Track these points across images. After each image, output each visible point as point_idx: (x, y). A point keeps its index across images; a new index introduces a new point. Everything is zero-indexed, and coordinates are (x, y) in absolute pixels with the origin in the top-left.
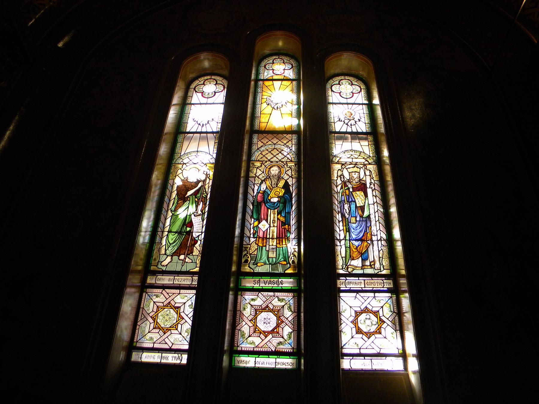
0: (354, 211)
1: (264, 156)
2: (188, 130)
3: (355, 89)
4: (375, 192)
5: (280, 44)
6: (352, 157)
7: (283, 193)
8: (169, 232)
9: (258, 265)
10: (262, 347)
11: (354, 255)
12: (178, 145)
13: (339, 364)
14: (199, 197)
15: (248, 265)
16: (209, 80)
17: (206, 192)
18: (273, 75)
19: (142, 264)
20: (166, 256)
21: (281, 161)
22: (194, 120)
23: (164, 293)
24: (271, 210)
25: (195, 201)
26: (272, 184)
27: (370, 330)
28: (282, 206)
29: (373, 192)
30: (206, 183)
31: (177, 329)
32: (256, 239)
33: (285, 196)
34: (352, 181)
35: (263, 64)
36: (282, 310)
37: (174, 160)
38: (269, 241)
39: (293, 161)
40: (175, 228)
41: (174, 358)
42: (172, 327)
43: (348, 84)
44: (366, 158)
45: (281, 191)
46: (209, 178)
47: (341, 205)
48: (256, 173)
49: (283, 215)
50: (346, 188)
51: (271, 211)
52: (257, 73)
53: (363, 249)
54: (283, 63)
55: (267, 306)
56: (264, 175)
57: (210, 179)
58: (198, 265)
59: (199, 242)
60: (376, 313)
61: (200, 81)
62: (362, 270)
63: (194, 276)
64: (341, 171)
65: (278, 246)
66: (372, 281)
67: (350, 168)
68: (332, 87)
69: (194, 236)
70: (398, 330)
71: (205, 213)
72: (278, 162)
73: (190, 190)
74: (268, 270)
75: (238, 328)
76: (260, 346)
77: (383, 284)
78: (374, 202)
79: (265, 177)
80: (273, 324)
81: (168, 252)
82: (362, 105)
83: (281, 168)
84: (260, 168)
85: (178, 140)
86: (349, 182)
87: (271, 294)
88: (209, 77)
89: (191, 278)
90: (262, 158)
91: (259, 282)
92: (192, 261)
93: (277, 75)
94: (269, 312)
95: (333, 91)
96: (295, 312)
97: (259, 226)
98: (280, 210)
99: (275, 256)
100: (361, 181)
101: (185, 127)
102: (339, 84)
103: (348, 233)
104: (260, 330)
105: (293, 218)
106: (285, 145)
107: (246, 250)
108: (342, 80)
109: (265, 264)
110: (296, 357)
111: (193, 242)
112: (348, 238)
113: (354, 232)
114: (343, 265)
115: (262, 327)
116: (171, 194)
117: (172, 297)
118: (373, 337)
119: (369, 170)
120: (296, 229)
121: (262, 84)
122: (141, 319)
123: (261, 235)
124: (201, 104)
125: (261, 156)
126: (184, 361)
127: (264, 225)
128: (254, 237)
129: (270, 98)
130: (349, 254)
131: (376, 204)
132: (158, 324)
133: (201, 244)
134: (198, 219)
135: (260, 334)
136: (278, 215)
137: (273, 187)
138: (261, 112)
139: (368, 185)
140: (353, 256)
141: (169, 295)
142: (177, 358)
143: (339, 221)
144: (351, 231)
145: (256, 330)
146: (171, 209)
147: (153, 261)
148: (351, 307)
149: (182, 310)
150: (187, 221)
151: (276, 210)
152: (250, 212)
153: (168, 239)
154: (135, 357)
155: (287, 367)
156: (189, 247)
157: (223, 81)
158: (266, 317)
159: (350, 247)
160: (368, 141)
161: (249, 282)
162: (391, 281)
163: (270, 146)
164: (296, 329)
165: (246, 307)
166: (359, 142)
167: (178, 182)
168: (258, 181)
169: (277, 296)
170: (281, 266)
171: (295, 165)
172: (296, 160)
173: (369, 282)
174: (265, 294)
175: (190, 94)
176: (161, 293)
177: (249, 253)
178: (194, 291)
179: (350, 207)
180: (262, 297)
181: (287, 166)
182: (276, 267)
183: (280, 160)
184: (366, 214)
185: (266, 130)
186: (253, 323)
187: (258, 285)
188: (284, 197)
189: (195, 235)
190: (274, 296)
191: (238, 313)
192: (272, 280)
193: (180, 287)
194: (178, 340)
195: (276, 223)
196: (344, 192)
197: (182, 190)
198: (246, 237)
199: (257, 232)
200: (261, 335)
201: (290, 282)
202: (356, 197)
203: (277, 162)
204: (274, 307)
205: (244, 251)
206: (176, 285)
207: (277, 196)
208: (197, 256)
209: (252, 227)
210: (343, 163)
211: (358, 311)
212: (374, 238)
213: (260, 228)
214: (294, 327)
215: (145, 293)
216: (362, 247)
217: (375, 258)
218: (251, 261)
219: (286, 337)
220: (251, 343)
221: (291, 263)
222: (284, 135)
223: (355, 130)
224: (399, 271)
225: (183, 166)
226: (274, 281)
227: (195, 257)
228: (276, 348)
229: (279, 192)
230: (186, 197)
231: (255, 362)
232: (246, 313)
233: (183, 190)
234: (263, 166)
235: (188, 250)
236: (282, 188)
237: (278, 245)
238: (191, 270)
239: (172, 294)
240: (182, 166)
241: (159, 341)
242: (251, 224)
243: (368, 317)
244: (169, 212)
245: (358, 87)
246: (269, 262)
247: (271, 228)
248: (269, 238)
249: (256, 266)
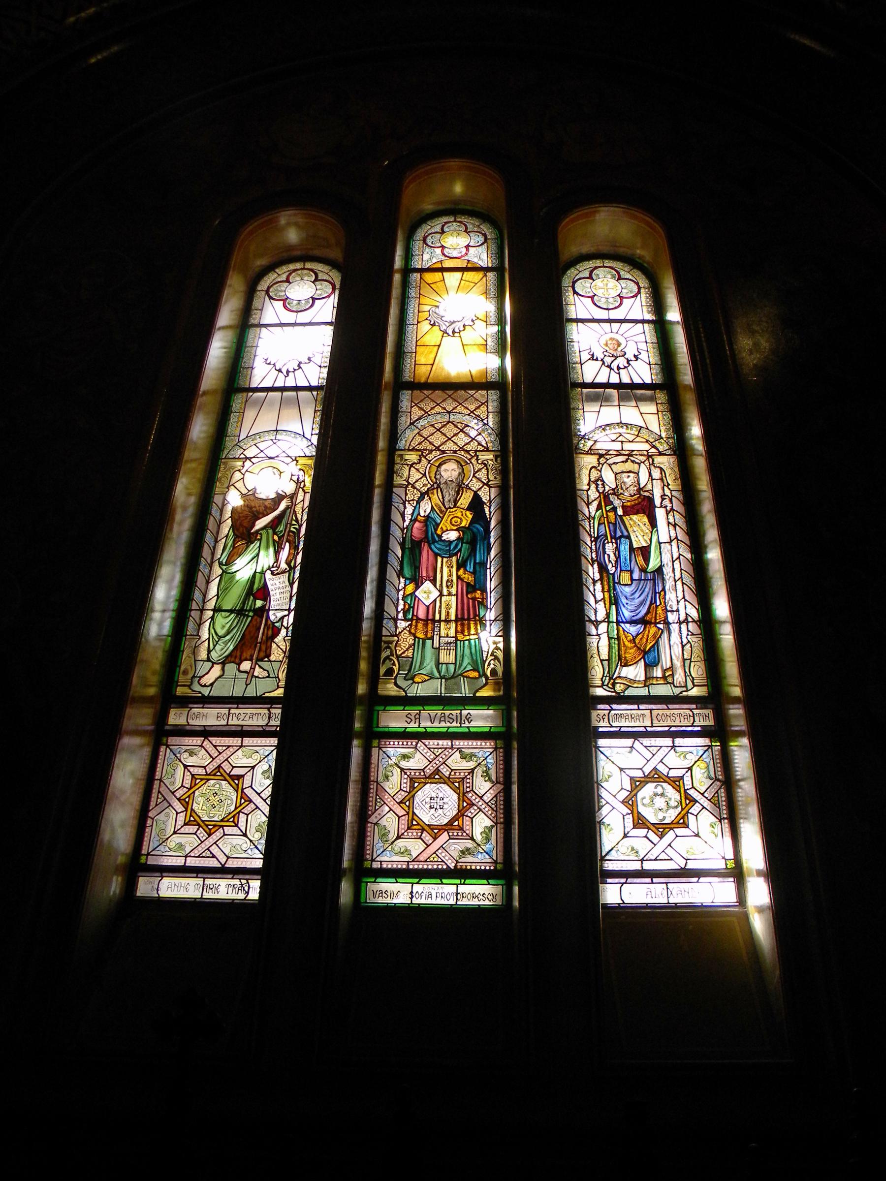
0: (628, 557)
1: (426, 439)
2: (254, 385)
3: (625, 289)
4: (674, 516)
5: (458, 188)
6: (621, 439)
7: (469, 522)
8: (217, 610)
9: (416, 680)
10: (426, 861)
11: (627, 655)
12: (233, 418)
13: (595, 894)
14: (282, 531)
15: (393, 681)
16: (299, 272)
17: (297, 521)
18: (443, 258)
19: (155, 684)
20: (210, 664)
21: (464, 450)
22: (268, 362)
23: (208, 746)
24: (443, 558)
25: (274, 541)
26: (444, 500)
27: (664, 818)
28: (468, 550)
29: (668, 516)
30: (298, 501)
31: (237, 825)
32: (410, 622)
33: (474, 527)
34: (621, 491)
35: (420, 234)
36: (469, 779)
37: (223, 450)
38: (440, 627)
39: (490, 448)
40: (231, 600)
41: (230, 889)
42: (226, 819)
43: (610, 276)
44: (652, 440)
45: (464, 514)
46: (302, 488)
47: (598, 546)
48: (409, 478)
49: (470, 568)
50: (608, 508)
51: (442, 561)
52: (408, 255)
53: (647, 641)
54: (466, 231)
55: (437, 771)
56: (427, 480)
57: (305, 493)
58: (282, 683)
59: (283, 632)
60: (676, 783)
61: (279, 275)
62: (647, 688)
63: (273, 706)
64: (598, 470)
65: (459, 638)
66: (668, 712)
67: (617, 463)
68: (576, 286)
69: (272, 618)
70: (724, 819)
71: (295, 567)
72: (458, 452)
73: (261, 516)
74: (439, 692)
75: (373, 819)
76: (421, 858)
77: (692, 718)
78: (670, 537)
79: (429, 486)
80: (451, 810)
81: (214, 655)
82: (641, 325)
83: (463, 464)
84: (417, 466)
85: (232, 406)
86: (616, 495)
87: (446, 743)
88: (298, 265)
89: (266, 711)
90: (420, 443)
91: (418, 717)
92: (268, 673)
93: (451, 258)
94: (440, 783)
95: (578, 294)
96: (500, 783)
97: (417, 593)
98: (463, 557)
99: (452, 660)
100: (642, 492)
101: (249, 377)
102: (590, 277)
103: (614, 607)
104: (421, 823)
106: (471, 414)
107: (389, 648)
108: (596, 268)
109: (432, 677)
110: (502, 882)
111: (270, 632)
112: (613, 618)
113: (627, 604)
114: (604, 678)
115: (426, 816)
116: (219, 526)
117: (224, 756)
118: (670, 835)
119: (658, 467)
121: (418, 279)
122: (157, 805)
123: (421, 614)
124: (281, 325)
125: (419, 439)
126: (254, 895)
127: (428, 593)
128: (405, 620)
129: (437, 311)
130: (617, 653)
131: (674, 543)
132: (194, 814)
133: (287, 636)
134: (281, 580)
135: (422, 833)
136: (458, 570)
137: (447, 506)
138: (417, 341)
139: (657, 502)
140: (625, 658)
141: (217, 750)
142: (237, 889)
143: (593, 580)
144: (622, 602)
145: (414, 824)
146: (220, 558)
147: (181, 676)
148: (621, 769)
149: (248, 782)
150: (256, 586)
151: (454, 559)
152: (396, 564)
153: (213, 625)
154: (145, 887)
155: (481, 903)
156: (260, 643)
157: (330, 273)
158: (434, 795)
159: (618, 638)
160: (657, 404)
161: (397, 719)
162: (709, 712)
163: (438, 417)
164: (502, 820)
165: (390, 774)
166: (637, 406)
167: (234, 500)
168: (413, 495)
169: (458, 748)
170: (466, 682)
171: (496, 457)
172: (497, 447)
173: (661, 714)
174: (432, 743)
175: (256, 303)
176: (201, 746)
177: (394, 653)
178: (274, 741)
179: (617, 549)
180: (425, 751)
181: (477, 460)
182: (455, 684)
183: (461, 448)
184: (653, 564)
185: (430, 381)
186: (407, 809)
187: (417, 725)
190: (452, 748)
191: (372, 787)
192: (447, 713)
193: (242, 733)
194: (239, 849)
195: (455, 586)
196: (604, 518)
197: (244, 517)
198: (388, 618)
199: (413, 608)
200: (424, 835)
201: (486, 718)
202: (631, 527)
203: (455, 452)
204: (453, 773)
205: (384, 650)
206: (233, 728)
207: (455, 528)
208: (280, 663)
209: (400, 597)
210: (600, 452)
211: (638, 779)
212: (672, 617)
213: (419, 599)
214: (496, 816)
215: (165, 747)
216: (645, 636)
217: (675, 661)
218: (400, 672)
219: (478, 837)
220: (402, 853)
221: (489, 674)
222: (470, 392)
223: (625, 380)
224: (726, 689)
225: (245, 464)
226: (451, 716)
227: (276, 665)
229: (461, 519)
230: (253, 534)
231: (411, 893)
232: (391, 786)
233: (246, 517)
234: (424, 461)
235: (260, 650)
236: (467, 509)
237: (460, 637)
238: (267, 695)
239: (224, 748)
240: (243, 464)
241: (196, 853)
242: (399, 591)
243: (659, 790)
244: (216, 565)
245: (633, 284)
246: (440, 675)
247: (443, 597)
248: (440, 621)
249: (412, 683)
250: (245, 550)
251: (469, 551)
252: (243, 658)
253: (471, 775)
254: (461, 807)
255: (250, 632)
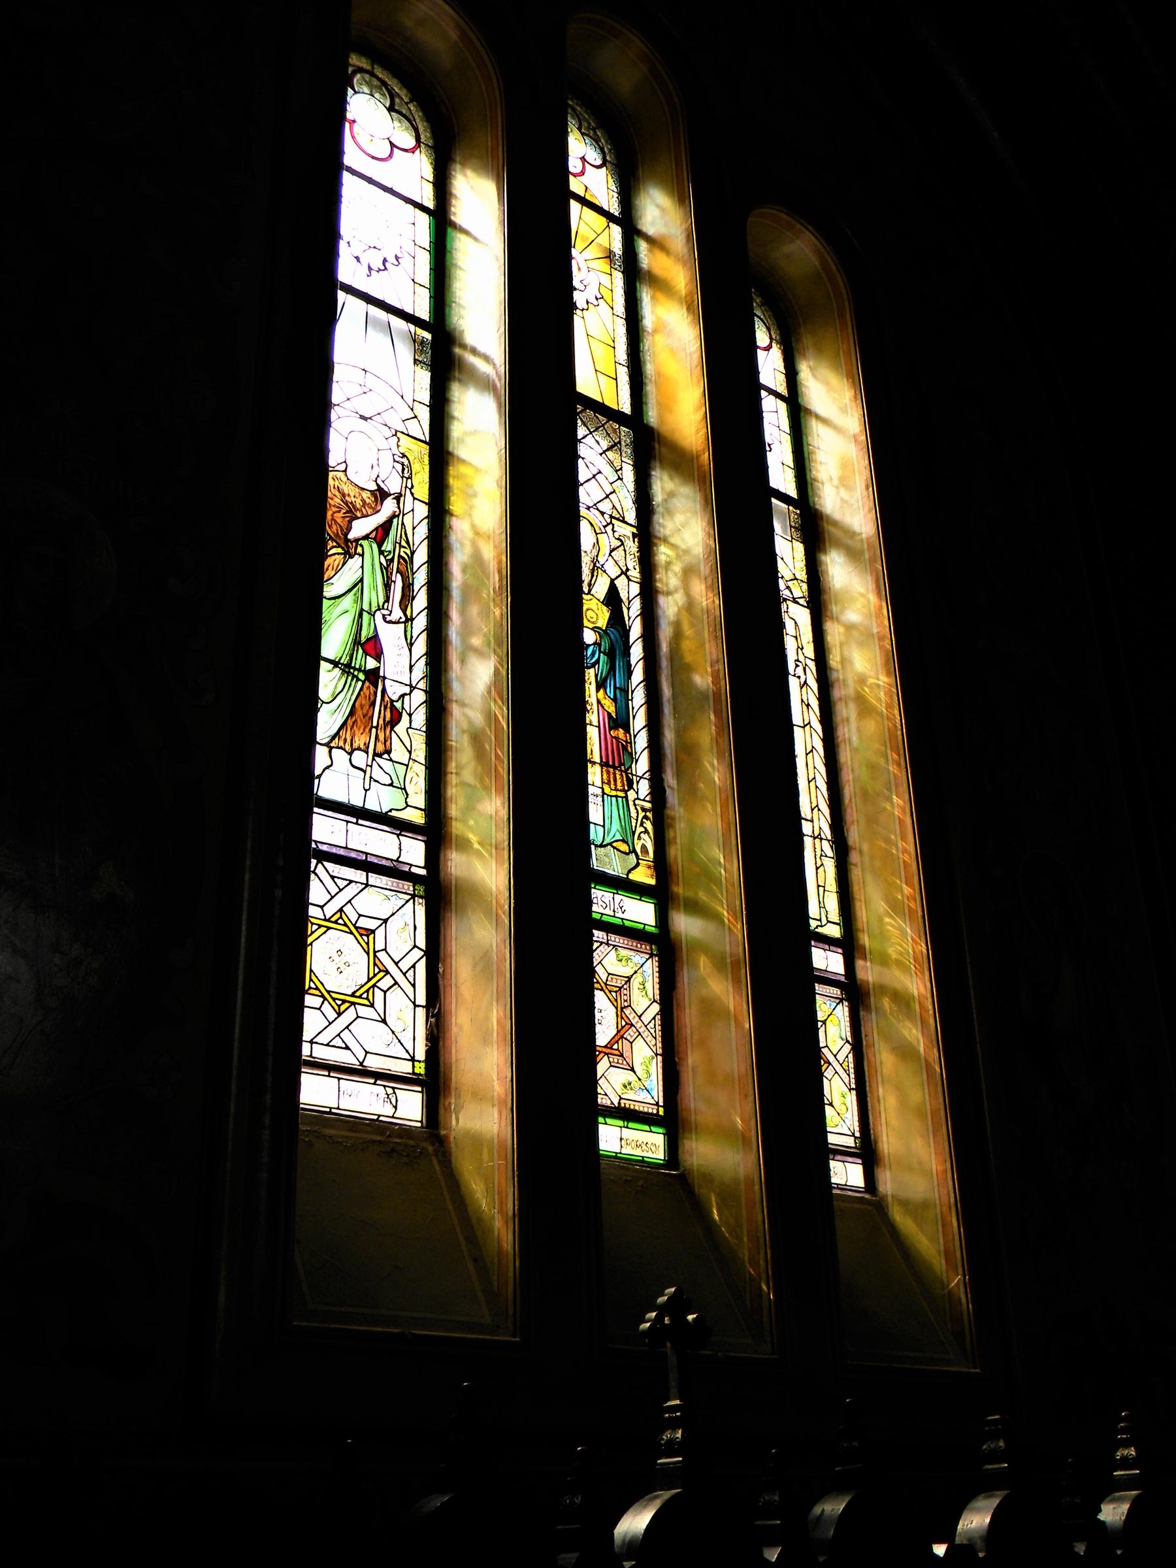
17: (408, 542)
45: (600, 609)
63: (403, 833)
105: (635, 711)
120: (646, 750)
136: (598, 691)
169: (614, 946)
188: (608, 635)
189: (394, 691)
190: (607, 944)
228: (621, 1098)
250: (343, 566)
251: (608, 666)
252: (355, 745)
253: (628, 984)
254: (620, 1027)
255: (362, 706)
